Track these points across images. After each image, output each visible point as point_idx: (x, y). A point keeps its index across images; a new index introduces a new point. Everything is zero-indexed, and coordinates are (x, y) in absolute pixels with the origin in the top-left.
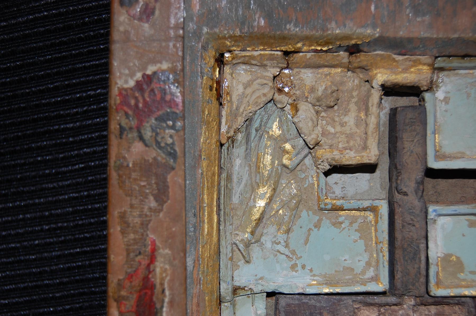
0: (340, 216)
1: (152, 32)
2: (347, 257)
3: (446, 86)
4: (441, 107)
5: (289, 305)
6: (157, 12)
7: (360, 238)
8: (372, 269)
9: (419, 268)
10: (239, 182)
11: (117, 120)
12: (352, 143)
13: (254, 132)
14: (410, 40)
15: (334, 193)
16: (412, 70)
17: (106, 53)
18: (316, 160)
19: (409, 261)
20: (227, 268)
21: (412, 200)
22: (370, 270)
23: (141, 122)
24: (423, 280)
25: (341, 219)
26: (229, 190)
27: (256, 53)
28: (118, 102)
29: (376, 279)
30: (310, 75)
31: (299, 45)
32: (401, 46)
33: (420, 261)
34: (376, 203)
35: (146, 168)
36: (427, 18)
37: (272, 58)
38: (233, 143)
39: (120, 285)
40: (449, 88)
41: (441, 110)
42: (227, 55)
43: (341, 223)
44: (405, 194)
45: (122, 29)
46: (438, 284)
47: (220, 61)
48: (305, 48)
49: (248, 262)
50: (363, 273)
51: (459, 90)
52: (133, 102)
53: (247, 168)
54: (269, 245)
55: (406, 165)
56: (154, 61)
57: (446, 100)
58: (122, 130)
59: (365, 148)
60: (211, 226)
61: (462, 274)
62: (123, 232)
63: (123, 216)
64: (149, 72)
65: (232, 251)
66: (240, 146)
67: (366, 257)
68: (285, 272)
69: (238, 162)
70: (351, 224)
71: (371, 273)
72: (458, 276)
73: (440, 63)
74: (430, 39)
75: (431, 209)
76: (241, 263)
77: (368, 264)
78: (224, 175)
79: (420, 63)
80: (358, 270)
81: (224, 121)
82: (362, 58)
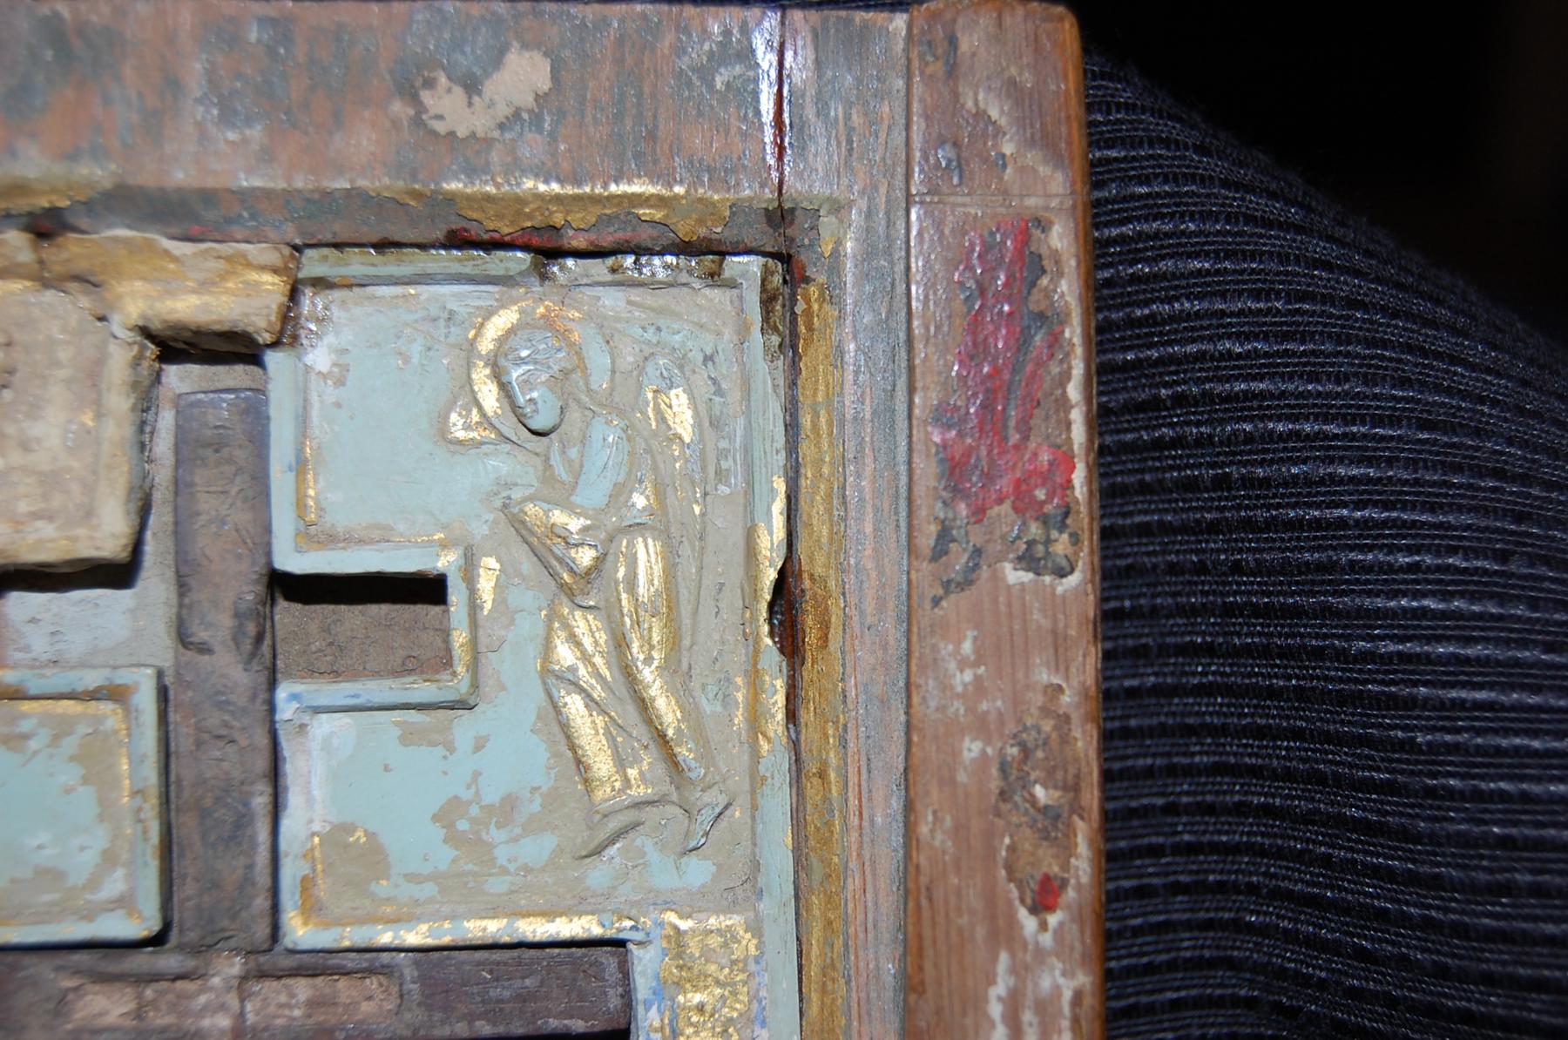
0: (25, 716)
2: (43, 837)
3: (337, 333)
4: (322, 396)
7: (86, 780)
8: (120, 873)
9: (250, 867)
12: (57, 501)
14: (208, 197)
15: (26, 649)
16: (230, 285)
21: (230, 670)
25: (25, 726)
29: (124, 903)
32: (189, 215)
34: (123, 677)
40: (347, 337)
41: (322, 402)
43: (26, 737)
44: (204, 649)
50: (94, 883)
51: (377, 345)
55: (205, 562)
59: (88, 514)
61: (384, 882)
67: (99, 839)
70: (56, 739)
71: (115, 885)
72: (373, 887)
73: (314, 264)
74: (268, 194)
75: (282, 694)
77: (109, 859)
79: (249, 265)
80: (77, 878)
82: (71, 251)
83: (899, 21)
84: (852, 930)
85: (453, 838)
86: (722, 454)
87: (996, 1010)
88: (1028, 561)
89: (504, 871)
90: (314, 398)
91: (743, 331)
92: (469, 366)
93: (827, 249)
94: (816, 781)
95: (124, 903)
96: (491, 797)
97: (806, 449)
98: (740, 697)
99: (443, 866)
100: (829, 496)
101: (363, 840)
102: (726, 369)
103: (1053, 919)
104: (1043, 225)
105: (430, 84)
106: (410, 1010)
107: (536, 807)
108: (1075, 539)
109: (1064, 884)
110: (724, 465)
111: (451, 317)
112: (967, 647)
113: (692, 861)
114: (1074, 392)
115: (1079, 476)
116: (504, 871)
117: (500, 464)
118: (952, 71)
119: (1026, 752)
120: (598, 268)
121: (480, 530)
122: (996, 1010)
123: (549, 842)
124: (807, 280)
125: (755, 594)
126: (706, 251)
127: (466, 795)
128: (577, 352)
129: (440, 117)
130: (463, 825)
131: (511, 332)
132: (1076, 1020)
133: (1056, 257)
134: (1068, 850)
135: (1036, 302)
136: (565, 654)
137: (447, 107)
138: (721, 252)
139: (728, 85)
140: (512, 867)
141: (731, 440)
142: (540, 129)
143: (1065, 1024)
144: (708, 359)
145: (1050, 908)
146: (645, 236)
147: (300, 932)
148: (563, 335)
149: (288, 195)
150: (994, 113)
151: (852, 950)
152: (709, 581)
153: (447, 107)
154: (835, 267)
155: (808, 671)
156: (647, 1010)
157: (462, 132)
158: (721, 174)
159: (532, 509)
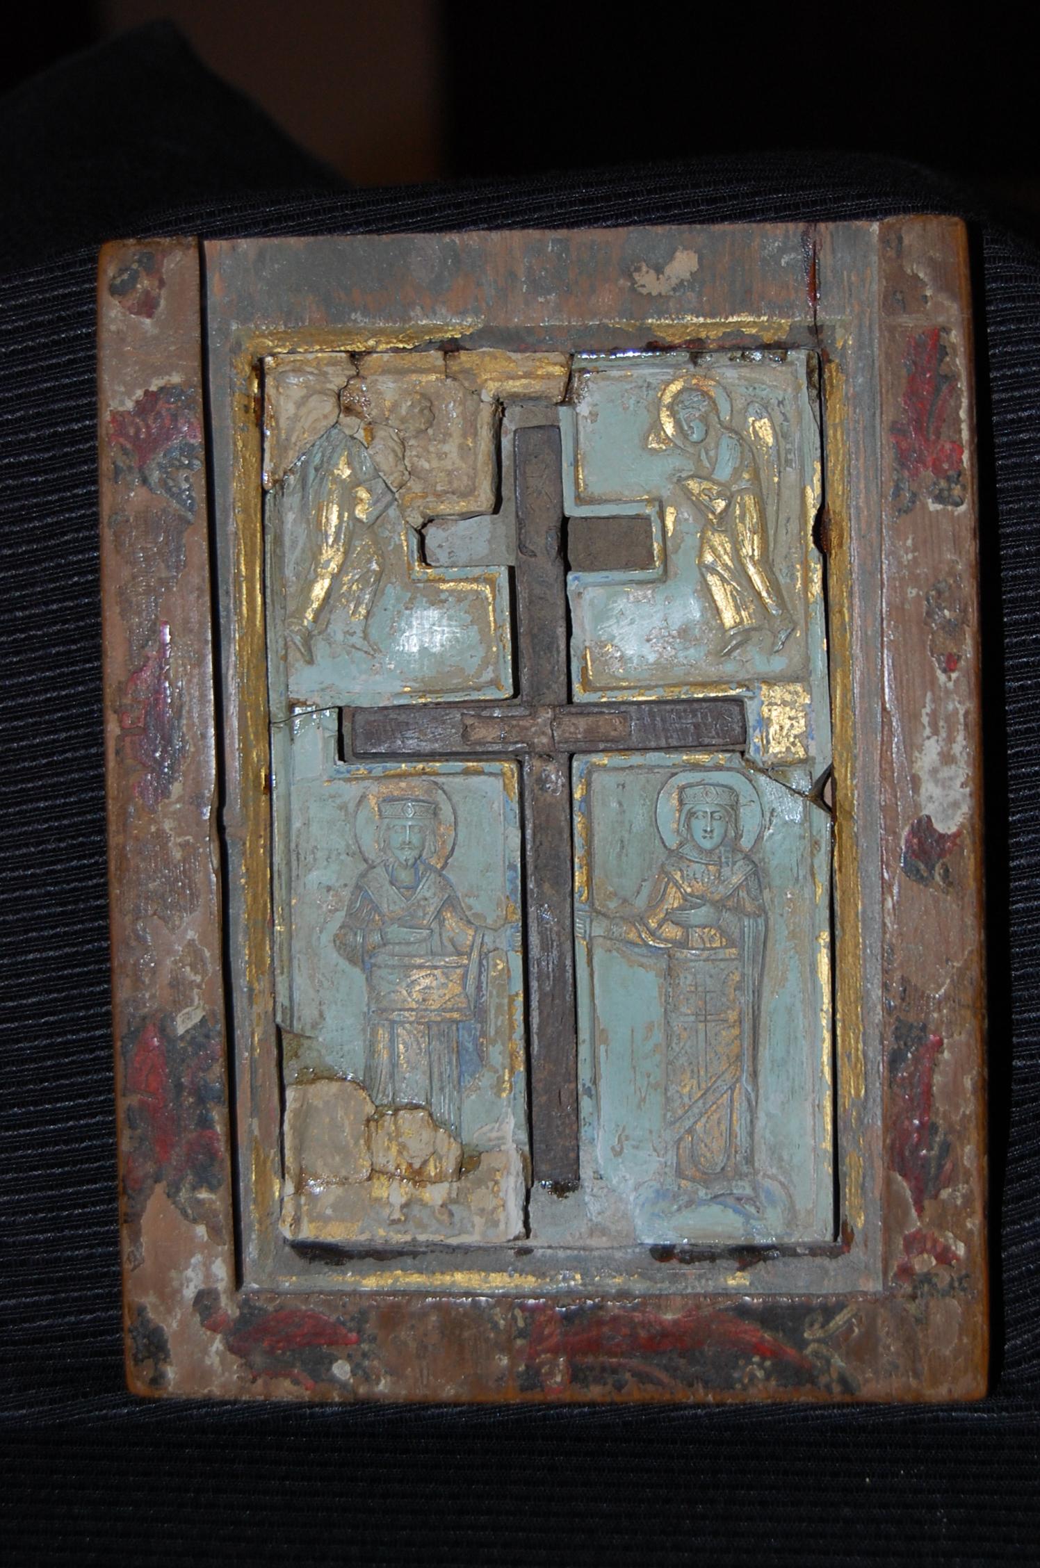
0: (442, 591)
1: (156, 331)
4: (586, 428)
5: (368, 723)
6: (163, 303)
8: (491, 668)
10: (293, 547)
11: (110, 456)
12: (456, 484)
13: (312, 472)
14: (530, 331)
17: (91, 364)
18: (402, 508)
20: (278, 672)
23: (143, 460)
25: (443, 597)
26: (280, 559)
27: (310, 356)
28: (112, 431)
30: (391, 385)
31: (371, 343)
33: (558, 652)
35: (149, 523)
36: (552, 297)
37: (333, 363)
38: (282, 488)
39: (121, 690)
40: (597, 397)
42: (269, 360)
45: (113, 328)
47: (259, 370)
48: (382, 347)
49: (311, 662)
51: (612, 401)
52: (132, 432)
53: (304, 526)
54: (340, 637)
56: (158, 371)
57: (594, 416)
58: (117, 471)
60: (252, 608)
62: (123, 614)
63: (121, 592)
64: (153, 388)
65: (286, 647)
66: (293, 493)
68: (364, 677)
69: (290, 517)
71: (488, 675)
76: (300, 664)
77: (485, 663)
78: (269, 538)
81: (267, 456)
82: (465, 359)
83: (875, 227)
86: (788, 451)
87: (925, 720)
88: (939, 498)
90: (581, 428)
91: (798, 389)
92: (659, 411)
93: (839, 344)
95: (495, 683)
97: (830, 447)
98: (799, 574)
100: (842, 470)
102: (789, 409)
103: (954, 675)
104: (947, 330)
105: (638, 269)
108: (964, 488)
109: (959, 657)
110: (789, 457)
111: (649, 385)
112: (909, 542)
114: (963, 414)
115: (965, 457)
117: (675, 462)
118: (900, 254)
119: (939, 593)
120: (724, 358)
121: (665, 493)
122: (925, 720)
124: (830, 361)
125: (806, 522)
126: (778, 348)
128: (713, 402)
129: (643, 286)
131: (680, 392)
132: (966, 725)
133: (954, 346)
134: (959, 642)
135: (943, 369)
136: (709, 558)
137: (648, 281)
138: (786, 350)
139: (787, 263)
141: (792, 443)
142: (693, 290)
143: (961, 727)
144: (780, 403)
145: (953, 670)
146: (747, 342)
148: (705, 394)
149: (569, 328)
150: (921, 275)
152: (782, 517)
153: (648, 281)
154: (843, 355)
155: (832, 562)
157: (654, 293)
158: (784, 309)
159: (693, 485)
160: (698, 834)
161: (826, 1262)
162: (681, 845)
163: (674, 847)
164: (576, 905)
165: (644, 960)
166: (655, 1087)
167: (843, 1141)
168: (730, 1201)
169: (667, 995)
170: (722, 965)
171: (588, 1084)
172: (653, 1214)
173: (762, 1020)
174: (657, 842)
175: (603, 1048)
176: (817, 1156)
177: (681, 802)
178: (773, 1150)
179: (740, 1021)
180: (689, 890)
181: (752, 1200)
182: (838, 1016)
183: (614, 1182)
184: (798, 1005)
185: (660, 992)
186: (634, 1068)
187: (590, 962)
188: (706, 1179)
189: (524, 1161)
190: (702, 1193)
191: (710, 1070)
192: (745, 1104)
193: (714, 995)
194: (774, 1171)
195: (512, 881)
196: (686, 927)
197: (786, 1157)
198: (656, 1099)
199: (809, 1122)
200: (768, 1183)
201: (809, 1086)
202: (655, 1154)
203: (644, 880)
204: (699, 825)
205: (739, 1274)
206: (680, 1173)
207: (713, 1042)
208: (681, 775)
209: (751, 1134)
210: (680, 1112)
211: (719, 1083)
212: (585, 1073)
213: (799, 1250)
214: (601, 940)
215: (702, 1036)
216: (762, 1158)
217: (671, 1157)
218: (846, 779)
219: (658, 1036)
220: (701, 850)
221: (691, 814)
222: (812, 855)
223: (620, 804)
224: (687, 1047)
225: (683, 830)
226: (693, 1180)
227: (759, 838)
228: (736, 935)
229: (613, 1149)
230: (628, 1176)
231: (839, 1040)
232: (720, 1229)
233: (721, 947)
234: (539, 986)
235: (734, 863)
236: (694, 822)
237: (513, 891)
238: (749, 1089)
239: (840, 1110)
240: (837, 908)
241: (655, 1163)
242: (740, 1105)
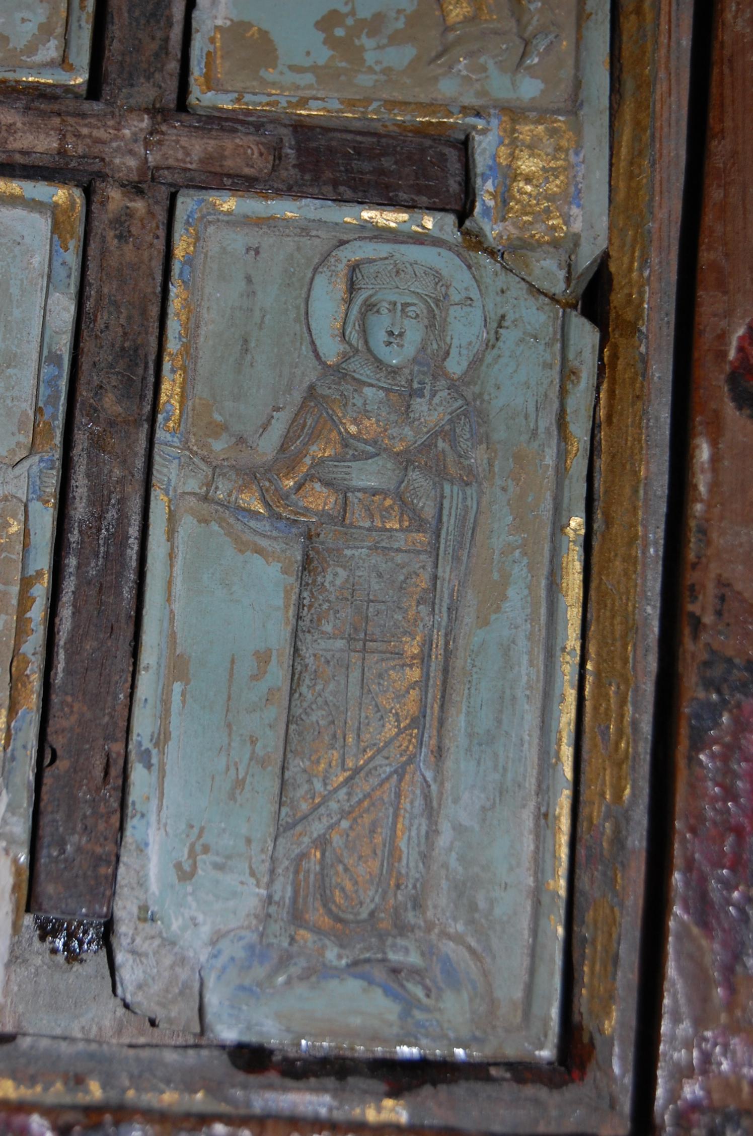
9: (167, 40)
19: (143, 22)
22: (48, 45)
24: (173, 66)
33: (170, 25)
46: (210, 83)
50: (31, 49)
61: (271, 70)
72: (262, 73)
77: (45, 30)
80: (19, 42)
84: (658, 124)
85: (331, 42)
89: (371, 70)
94: (633, 17)
96: (365, 13)
99: (321, 62)
101: (256, 36)
106: (287, 169)
107: (400, 24)
113: (420, 405)
116: (371, 70)
123: (408, 52)
127: (345, 10)
130: (340, 32)
140: (377, 68)
147: (202, 97)
151: (657, 140)
156: (484, 181)
160: (379, 337)
161: (542, 1093)
162: (346, 357)
163: (331, 360)
164: (160, 434)
165: (264, 543)
166: (263, 763)
167: (584, 882)
168: (379, 973)
169: (300, 605)
170: (399, 558)
171: (147, 744)
172: (242, 988)
173: (459, 663)
174: (306, 349)
175: (177, 687)
176: (537, 904)
177: (352, 287)
178: (463, 891)
179: (424, 658)
180: (353, 429)
181: (416, 973)
182: (589, 666)
183: (175, 926)
184: (522, 643)
185: (287, 597)
186: (229, 726)
187: (171, 533)
188: (342, 929)
189: (18, 873)
190: (331, 954)
191: (366, 737)
192: (419, 802)
193: (382, 607)
194: (460, 927)
195: (52, 382)
196: (344, 492)
197: (482, 904)
198: (266, 783)
199: (528, 844)
200: (449, 947)
201: (531, 783)
202: (252, 881)
203: (277, 409)
204: (380, 326)
205: (389, 1103)
206: (297, 917)
207: (374, 687)
208: (358, 243)
209: (425, 857)
210: (304, 807)
211: (379, 760)
212: (144, 725)
213: (493, 1071)
214: (192, 500)
215: (355, 675)
216: (440, 902)
217: (283, 890)
218: (630, 269)
219: (277, 675)
220: (379, 363)
221: (370, 307)
222: (563, 393)
223: (249, 280)
224: (326, 694)
225: (354, 336)
226: (317, 930)
227: (476, 362)
228: (429, 512)
229: (178, 866)
230: (200, 918)
231: (588, 704)
232: (356, 1021)
233: (402, 529)
234: (79, 567)
235: (434, 394)
236: (372, 318)
237: (53, 400)
238: (429, 775)
239: (583, 826)
240: (600, 485)
241: (251, 897)
242: (412, 803)
